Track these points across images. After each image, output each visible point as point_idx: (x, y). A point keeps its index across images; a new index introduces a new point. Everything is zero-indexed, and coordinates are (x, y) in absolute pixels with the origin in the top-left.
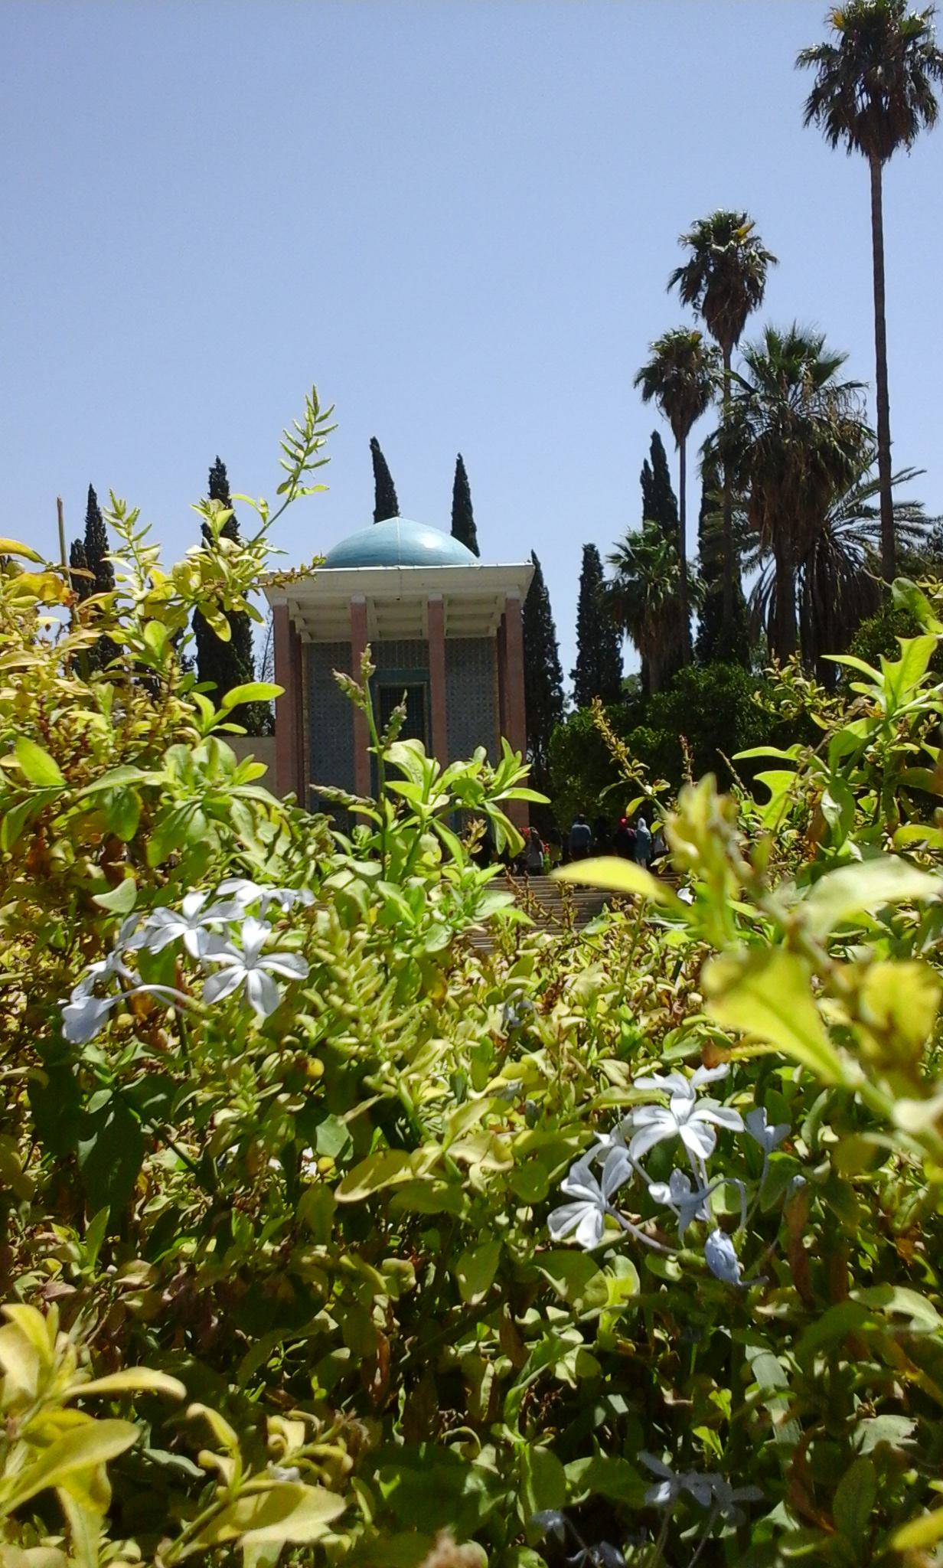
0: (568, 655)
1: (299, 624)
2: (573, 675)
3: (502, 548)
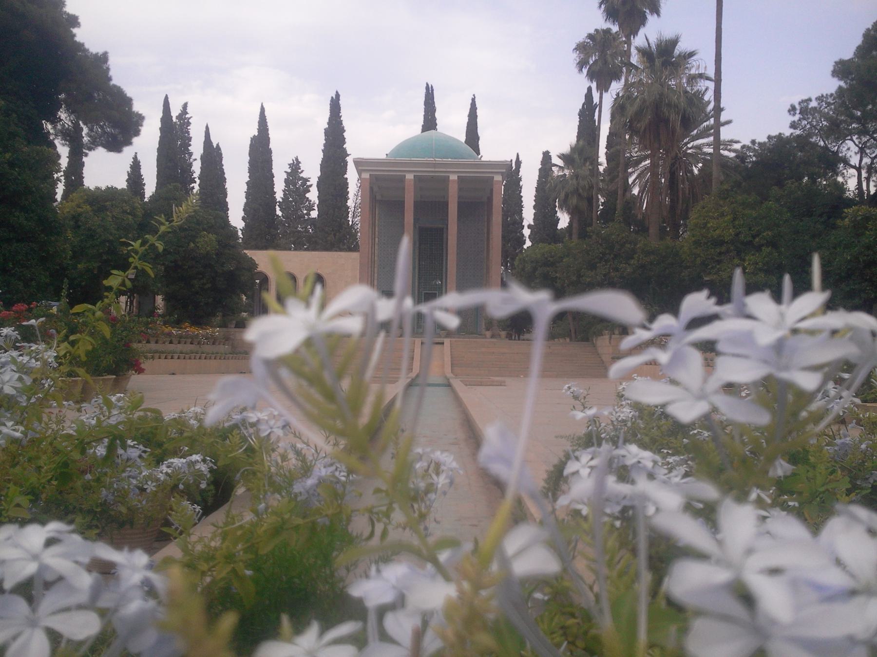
0: (528, 215)
2: (529, 227)
3: (493, 150)
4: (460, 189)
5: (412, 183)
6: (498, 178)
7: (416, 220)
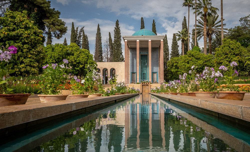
1: (129, 44)
4: (152, 44)
5: (139, 42)
6: (162, 40)
7: (140, 53)
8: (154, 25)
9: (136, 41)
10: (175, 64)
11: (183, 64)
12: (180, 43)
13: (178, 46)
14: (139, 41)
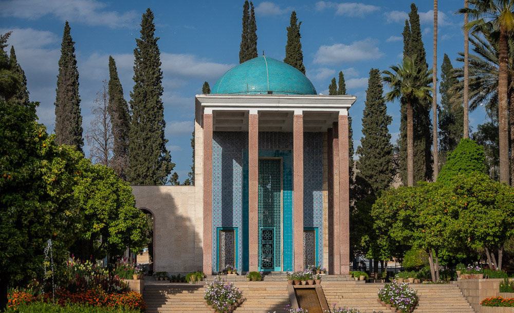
8: (294, 35)
9: (245, 114)
10: (402, 214)
11: (438, 217)
12: (394, 109)
13: (389, 119)
14: (256, 113)
